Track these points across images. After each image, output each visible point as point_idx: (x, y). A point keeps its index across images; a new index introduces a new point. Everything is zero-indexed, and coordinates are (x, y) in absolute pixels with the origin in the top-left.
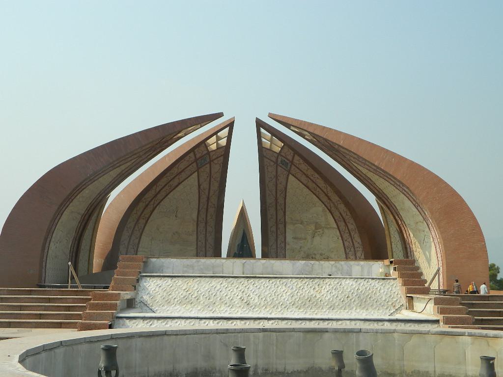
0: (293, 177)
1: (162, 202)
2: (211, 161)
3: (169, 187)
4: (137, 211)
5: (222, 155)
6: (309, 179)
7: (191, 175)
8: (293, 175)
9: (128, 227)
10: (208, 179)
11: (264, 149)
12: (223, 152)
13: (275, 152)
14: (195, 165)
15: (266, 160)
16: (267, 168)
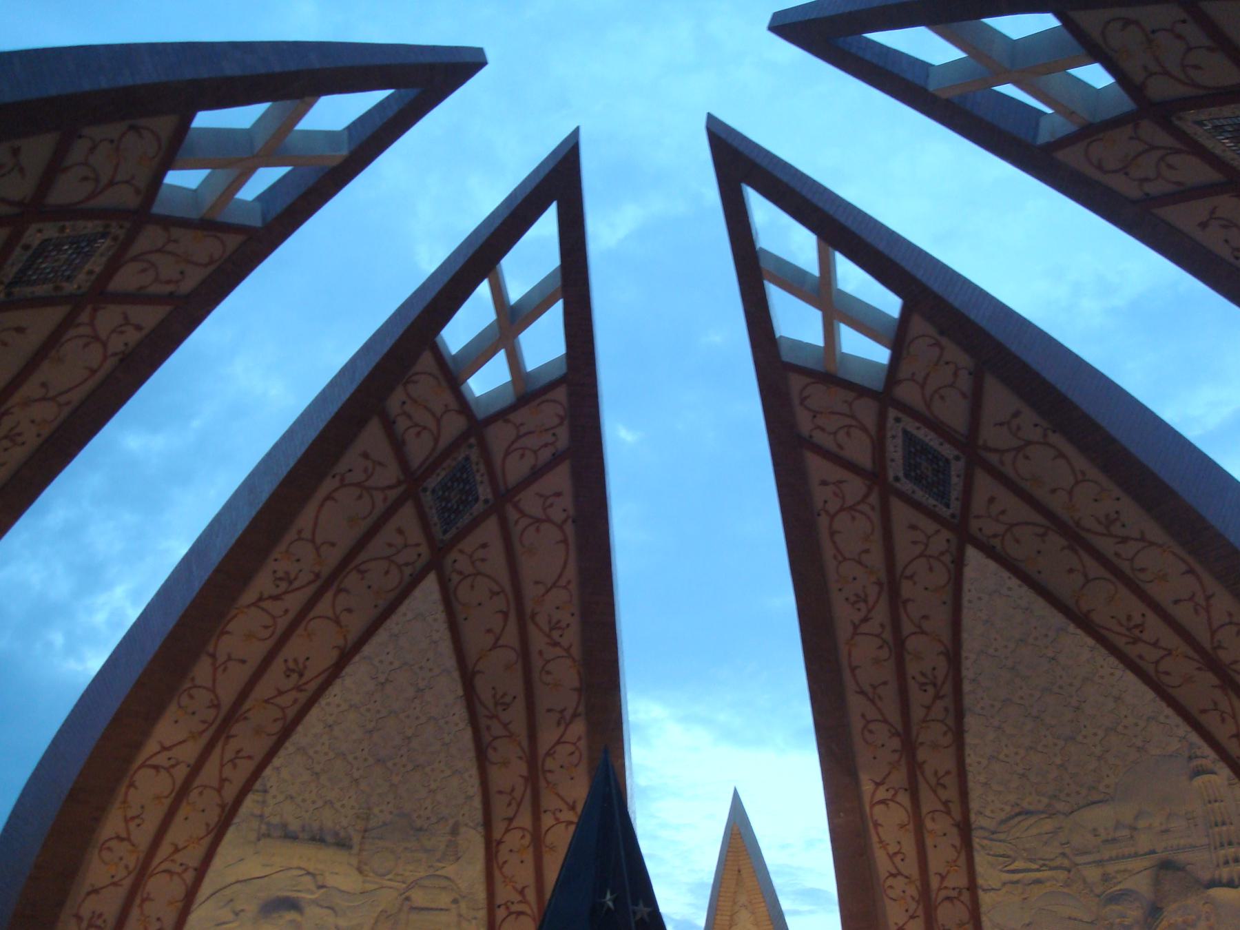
0: (992, 565)
1: (268, 771)
2: (504, 497)
3: (288, 673)
4: (127, 820)
5: (556, 459)
6: (1090, 563)
7: (404, 593)
8: (990, 552)
9: (85, 912)
10: (511, 636)
11: (796, 383)
12: (563, 439)
13: (861, 391)
14: (407, 516)
15: (817, 467)
16: (832, 534)
